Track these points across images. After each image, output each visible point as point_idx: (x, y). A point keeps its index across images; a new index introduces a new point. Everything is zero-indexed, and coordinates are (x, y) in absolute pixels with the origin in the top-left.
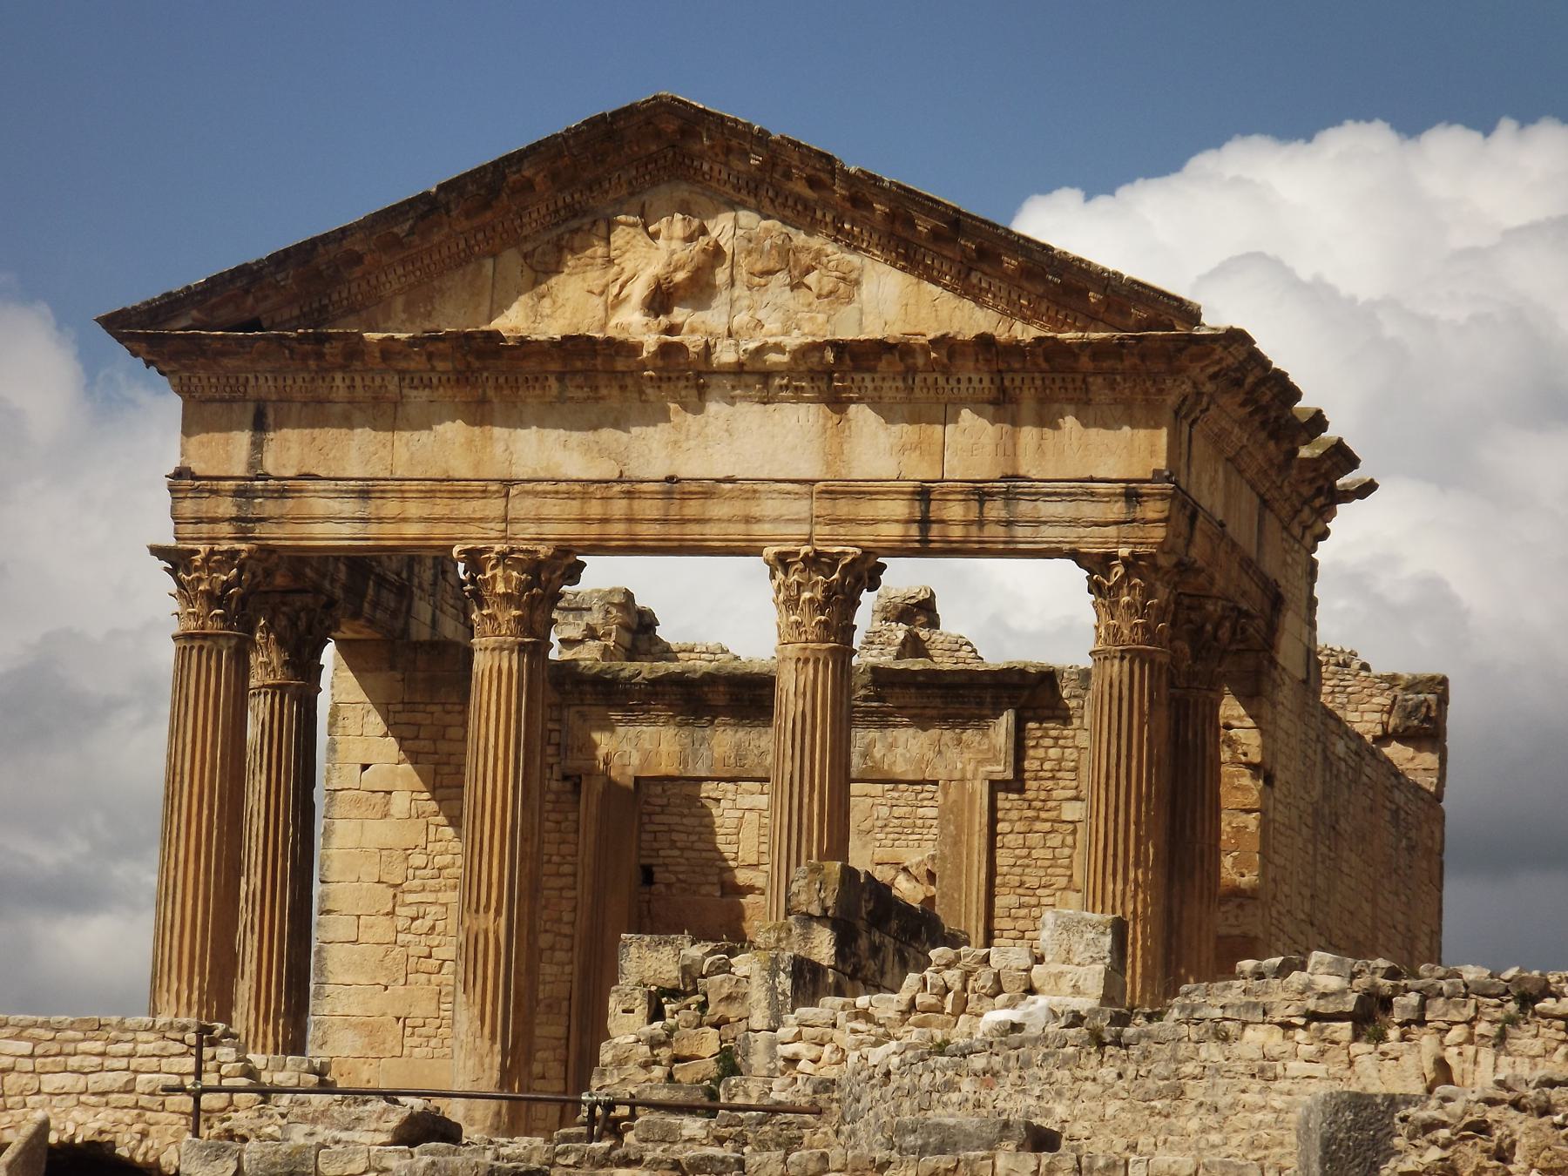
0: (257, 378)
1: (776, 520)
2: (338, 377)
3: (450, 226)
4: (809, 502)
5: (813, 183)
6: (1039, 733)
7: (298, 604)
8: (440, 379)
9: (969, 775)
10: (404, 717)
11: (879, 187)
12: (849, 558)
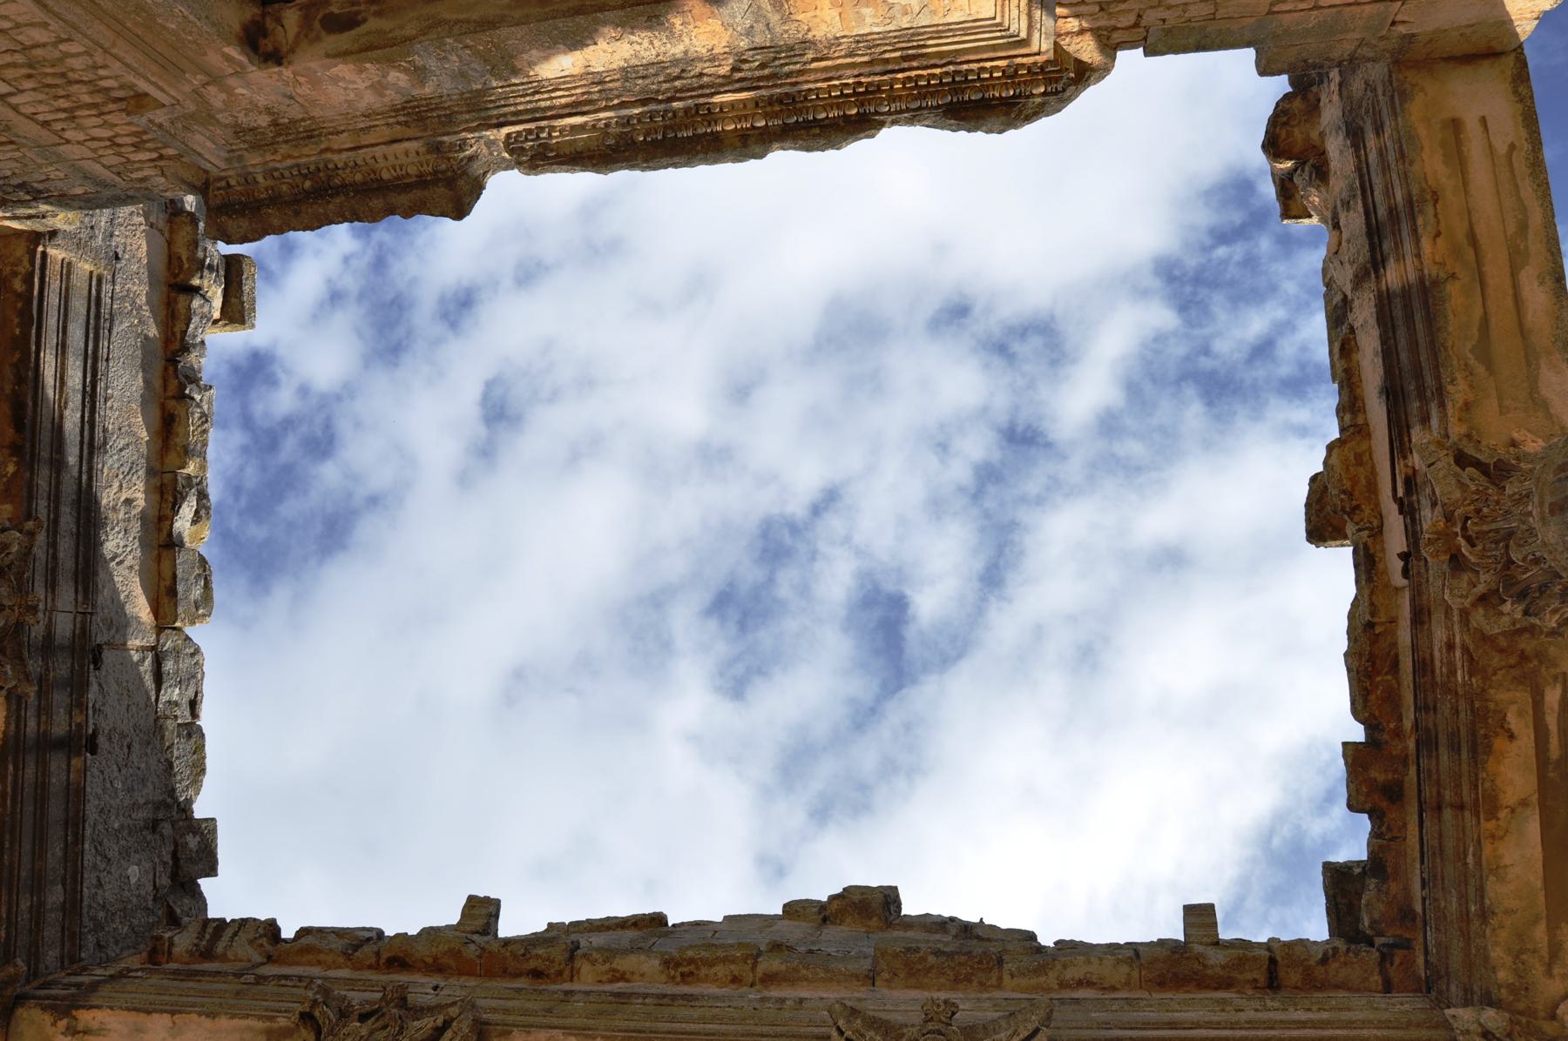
9: (212, 89)
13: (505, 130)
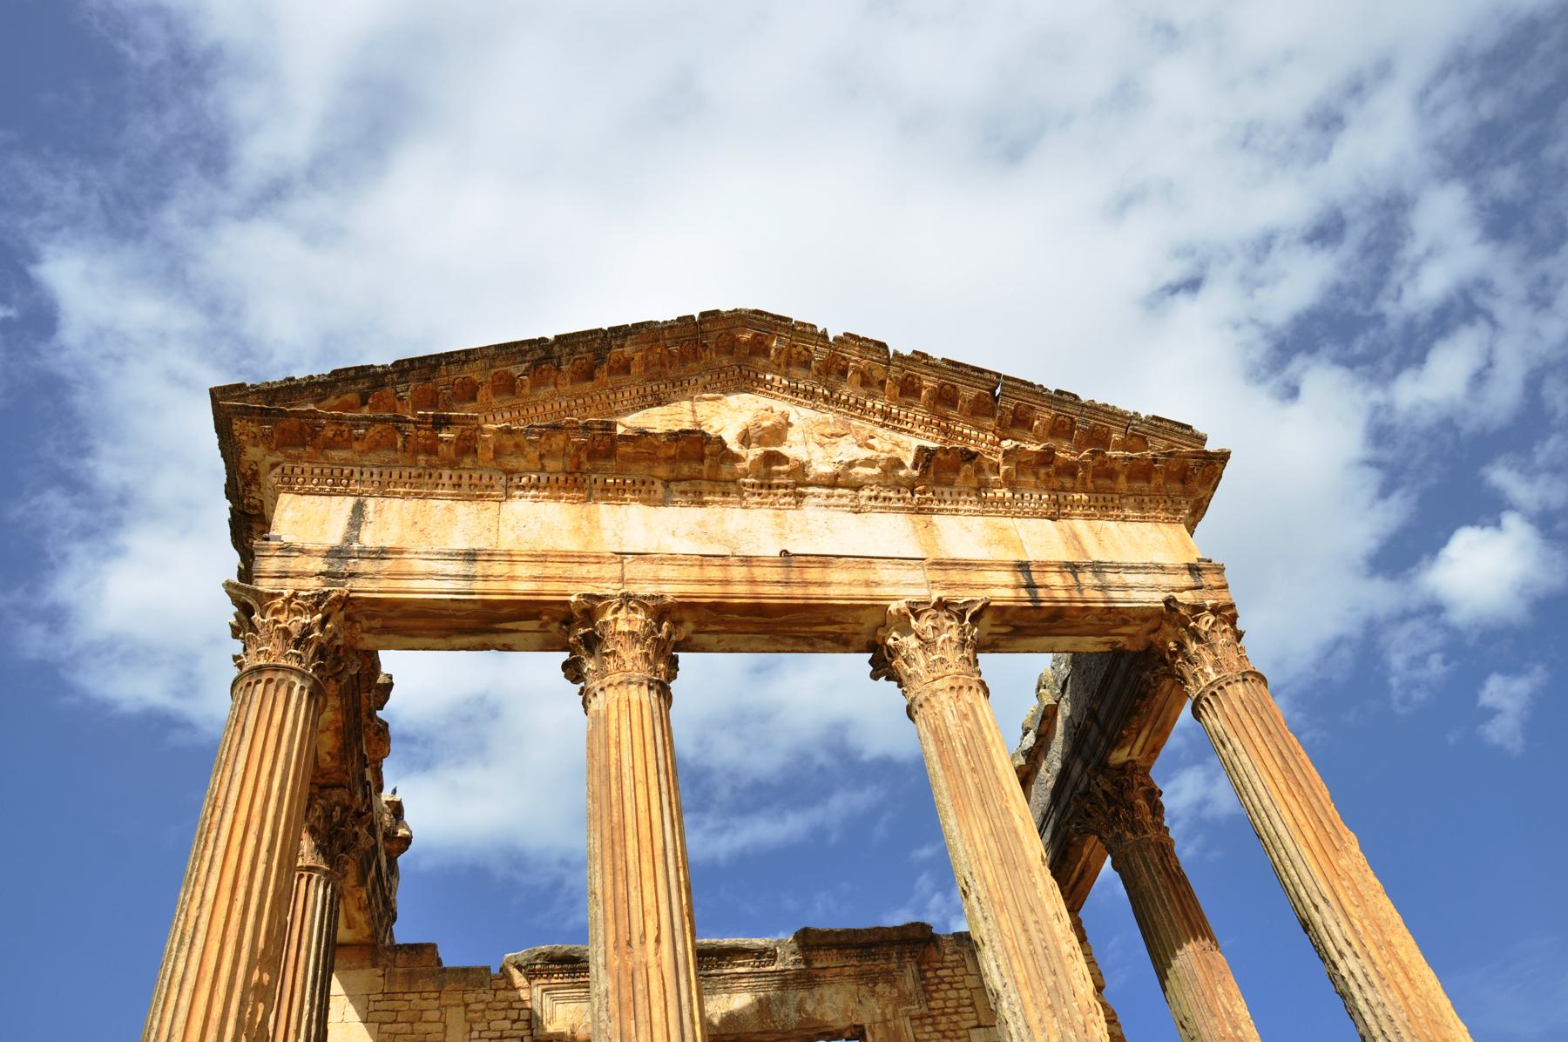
0: (362, 474)
1: (894, 584)
2: (446, 473)
3: (556, 385)
4: (922, 572)
5: (866, 382)
6: (936, 981)
7: (335, 799)
8: (548, 478)
9: (888, 1017)
10: (384, 1005)
11: (931, 365)
12: (980, 605)
13: (772, 968)
